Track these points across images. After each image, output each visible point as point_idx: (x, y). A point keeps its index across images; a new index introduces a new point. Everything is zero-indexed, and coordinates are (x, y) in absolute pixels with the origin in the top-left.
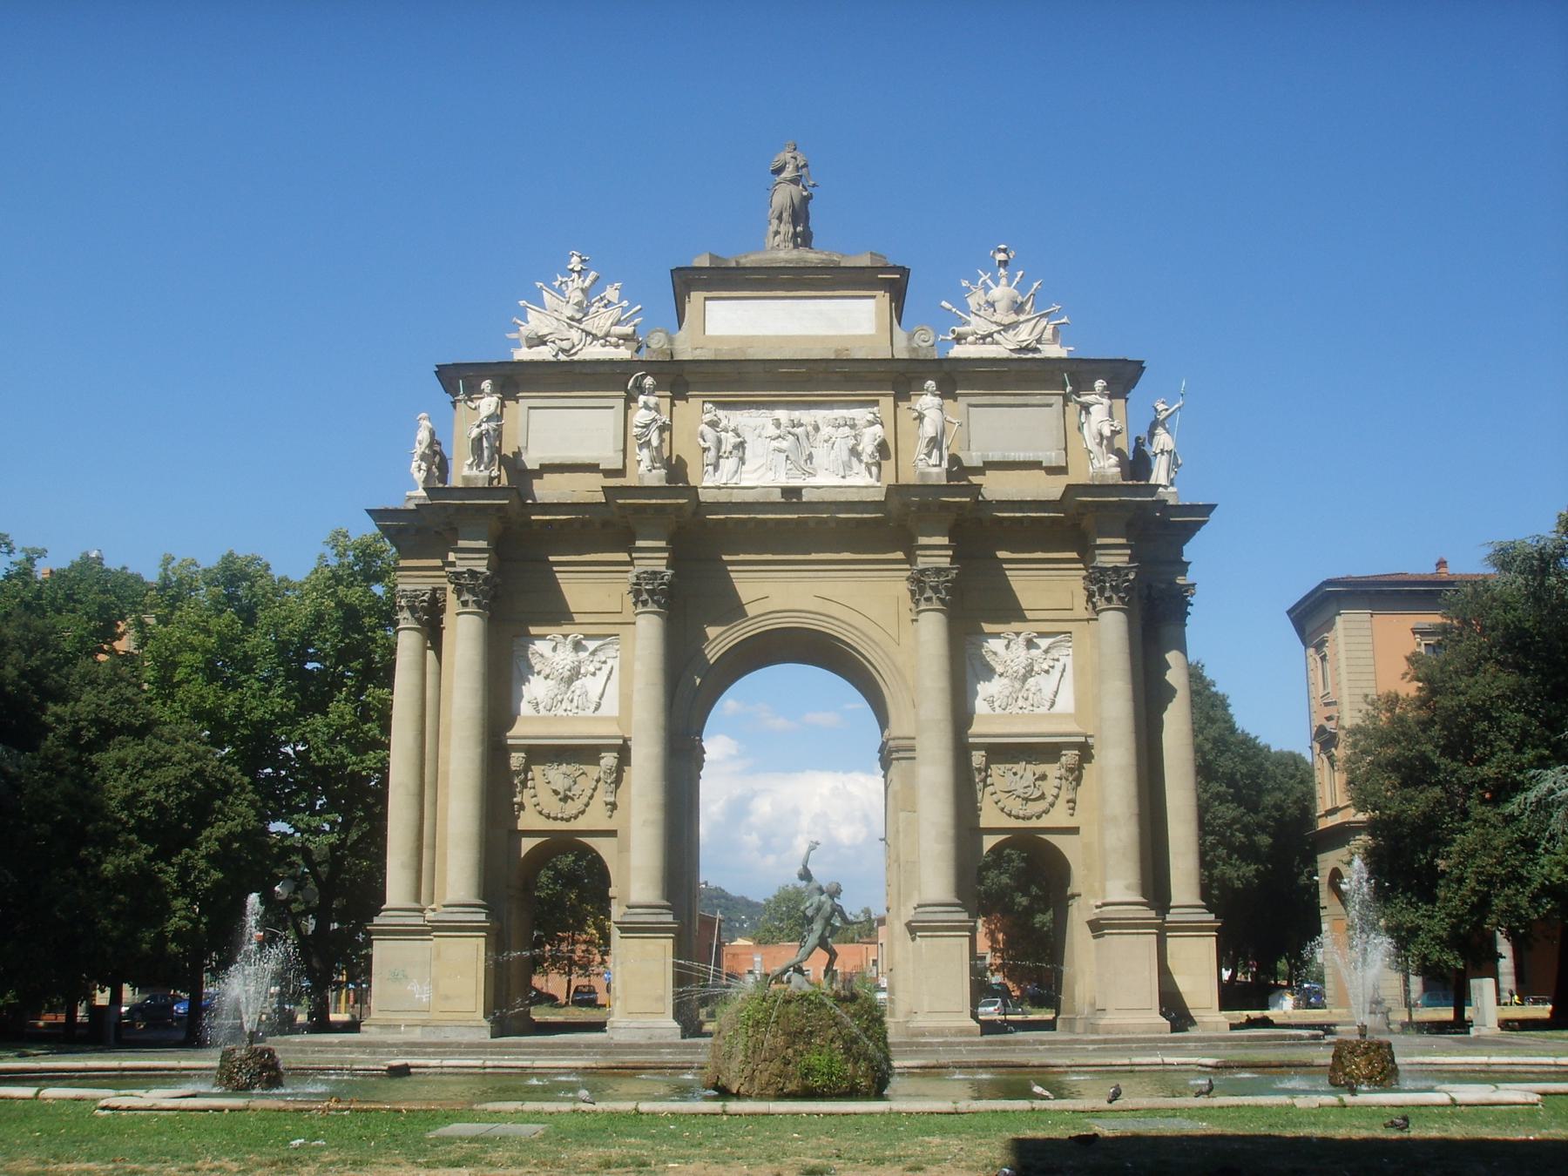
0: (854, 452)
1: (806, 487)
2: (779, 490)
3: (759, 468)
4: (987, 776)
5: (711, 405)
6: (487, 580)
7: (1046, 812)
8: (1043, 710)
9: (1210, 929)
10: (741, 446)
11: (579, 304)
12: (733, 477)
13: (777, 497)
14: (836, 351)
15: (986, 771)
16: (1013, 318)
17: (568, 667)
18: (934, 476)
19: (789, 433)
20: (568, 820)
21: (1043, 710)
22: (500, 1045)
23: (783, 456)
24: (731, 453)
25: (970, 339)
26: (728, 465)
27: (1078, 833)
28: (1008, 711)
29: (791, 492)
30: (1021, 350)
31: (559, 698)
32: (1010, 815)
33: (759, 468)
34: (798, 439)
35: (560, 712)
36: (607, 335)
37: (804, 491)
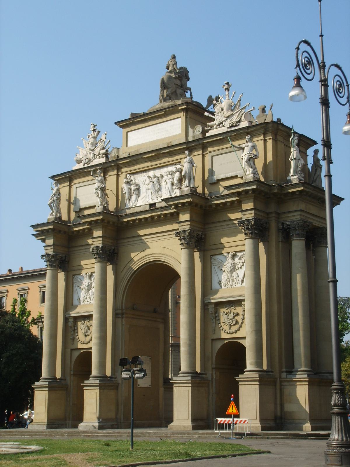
0: (173, 184)
1: (157, 202)
2: (149, 205)
3: (144, 197)
4: (216, 317)
5: (129, 175)
6: (53, 256)
7: (239, 330)
8: (239, 285)
9: (305, 381)
10: (138, 189)
11: (92, 143)
12: (134, 203)
13: (148, 208)
14: (168, 143)
15: (216, 313)
16: (230, 113)
17: (86, 285)
18: (186, 191)
19: (151, 182)
20: (87, 344)
21: (239, 285)
22: (266, 434)
23: (150, 191)
24: (133, 193)
25: (215, 127)
26: (134, 197)
27: (245, 339)
28: (226, 287)
29: (152, 205)
30: (232, 126)
31: (85, 297)
32: (228, 333)
33: (144, 197)
34: (154, 183)
35: (86, 303)
36: (99, 154)
37: (157, 204)
